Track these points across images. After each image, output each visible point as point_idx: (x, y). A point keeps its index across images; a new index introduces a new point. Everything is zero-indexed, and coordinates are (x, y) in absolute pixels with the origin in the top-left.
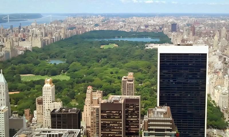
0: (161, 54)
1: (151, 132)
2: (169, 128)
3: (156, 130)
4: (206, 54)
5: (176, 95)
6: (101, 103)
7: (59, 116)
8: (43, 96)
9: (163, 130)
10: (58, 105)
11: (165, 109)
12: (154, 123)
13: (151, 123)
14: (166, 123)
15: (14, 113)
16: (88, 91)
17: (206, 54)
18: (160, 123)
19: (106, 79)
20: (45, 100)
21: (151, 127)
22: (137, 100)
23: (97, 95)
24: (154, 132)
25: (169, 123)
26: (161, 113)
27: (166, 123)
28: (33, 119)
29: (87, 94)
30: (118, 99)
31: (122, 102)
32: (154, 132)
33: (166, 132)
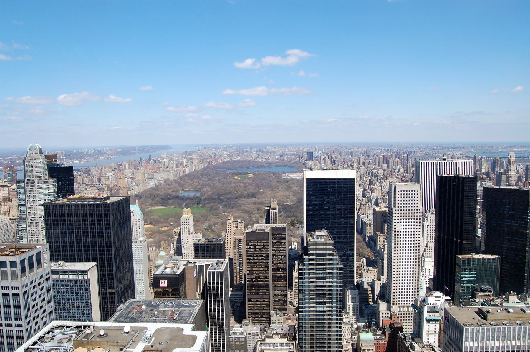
0: (307, 179)
1: (311, 257)
2: (331, 252)
3: (317, 255)
4: (354, 179)
5: (323, 223)
6: (247, 233)
7: (203, 246)
8: (181, 227)
9: (325, 255)
10: (199, 238)
11: (324, 233)
12: (315, 247)
13: (311, 247)
14: (327, 247)
15: (151, 246)
16: (229, 221)
17: (354, 179)
18: (321, 247)
19: (243, 210)
20: (184, 231)
21: (311, 252)
22: (284, 229)
23: (239, 225)
24: (314, 257)
25: (331, 247)
26: (321, 236)
27: (327, 247)
28: (171, 252)
29: (228, 225)
30: (264, 227)
31: (268, 230)
32: (314, 257)
33: (327, 257)
